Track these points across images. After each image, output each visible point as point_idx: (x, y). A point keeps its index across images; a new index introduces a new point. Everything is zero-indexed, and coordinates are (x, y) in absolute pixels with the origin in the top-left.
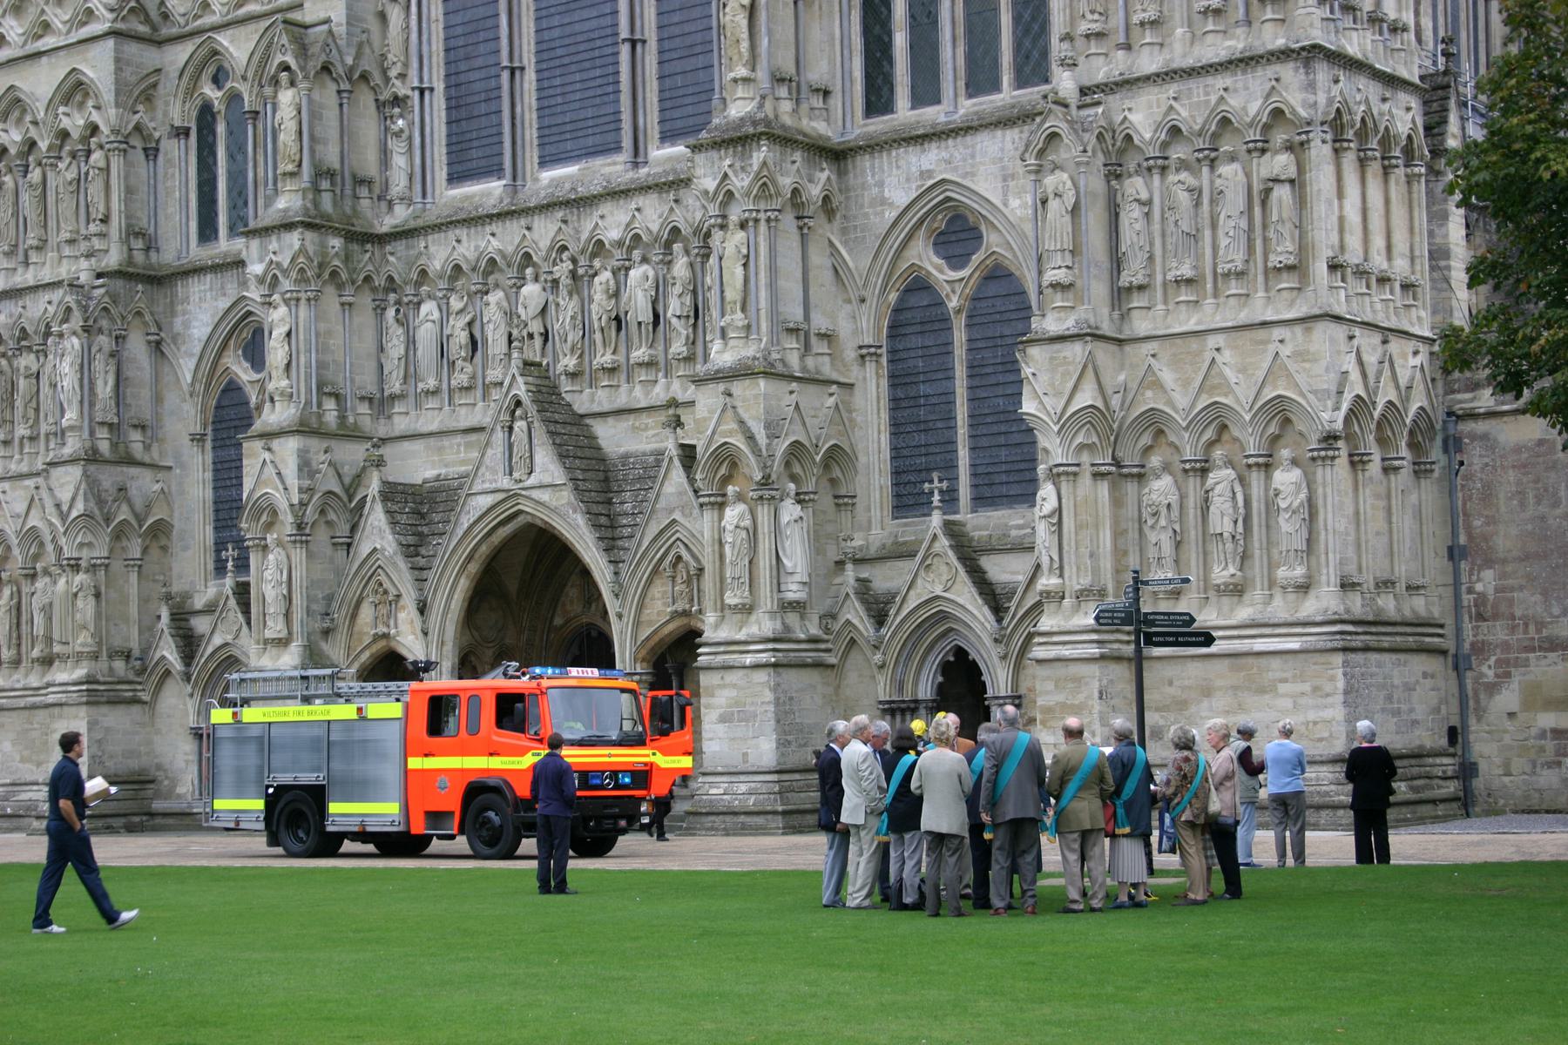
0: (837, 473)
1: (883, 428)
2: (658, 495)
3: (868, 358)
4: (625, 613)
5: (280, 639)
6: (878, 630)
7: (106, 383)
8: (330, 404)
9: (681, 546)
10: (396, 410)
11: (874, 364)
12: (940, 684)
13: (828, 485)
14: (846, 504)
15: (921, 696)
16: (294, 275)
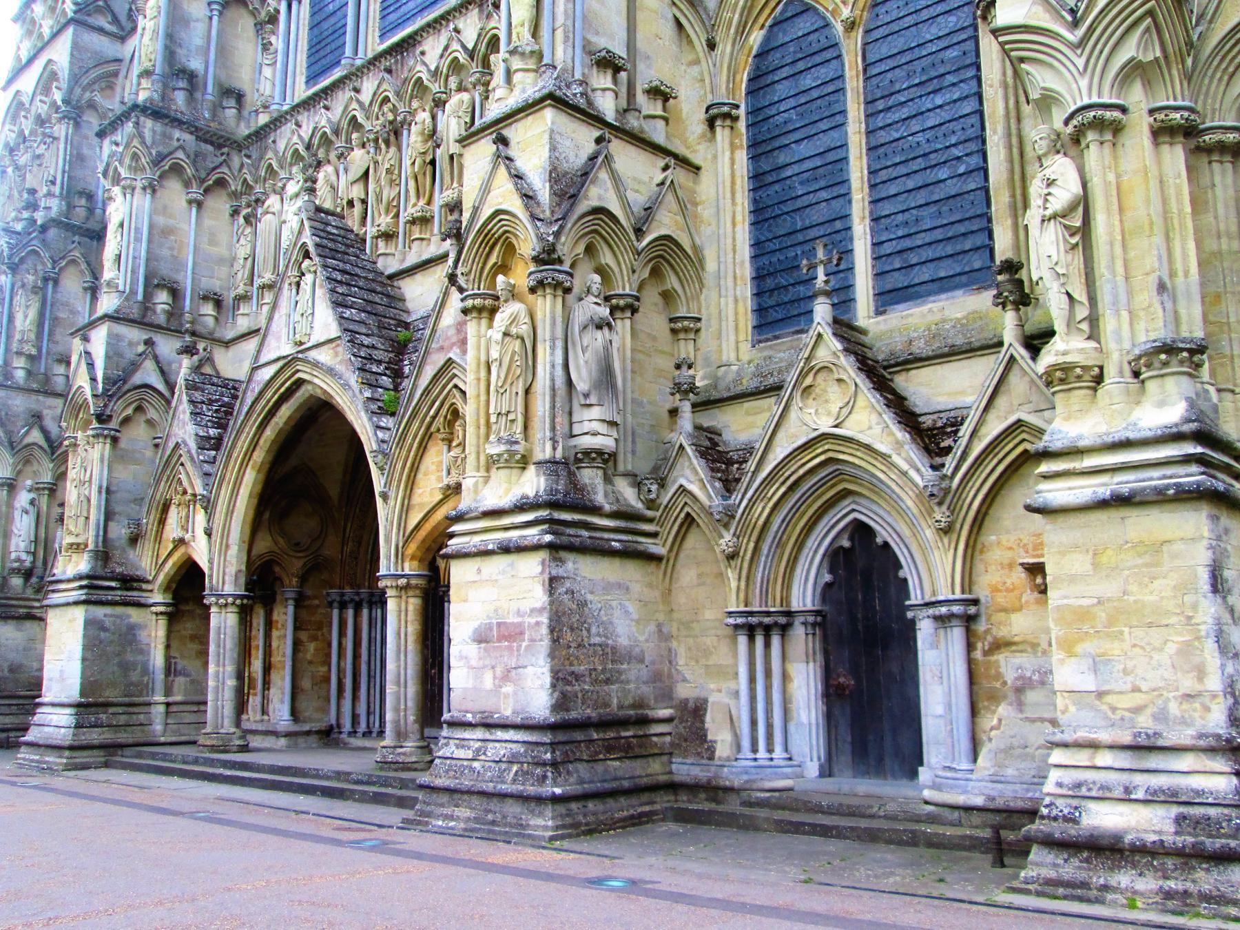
0: (672, 282)
1: (739, 218)
2: (434, 331)
3: (718, 122)
4: (392, 494)
5: (78, 545)
6: (725, 498)
7: (26, 317)
8: (163, 297)
9: (458, 394)
10: (241, 311)
11: (727, 131)
12: (828, 586)
13: (659, 300)
14: (686, 330)
15: (796, 605)
16: (127, 161)
